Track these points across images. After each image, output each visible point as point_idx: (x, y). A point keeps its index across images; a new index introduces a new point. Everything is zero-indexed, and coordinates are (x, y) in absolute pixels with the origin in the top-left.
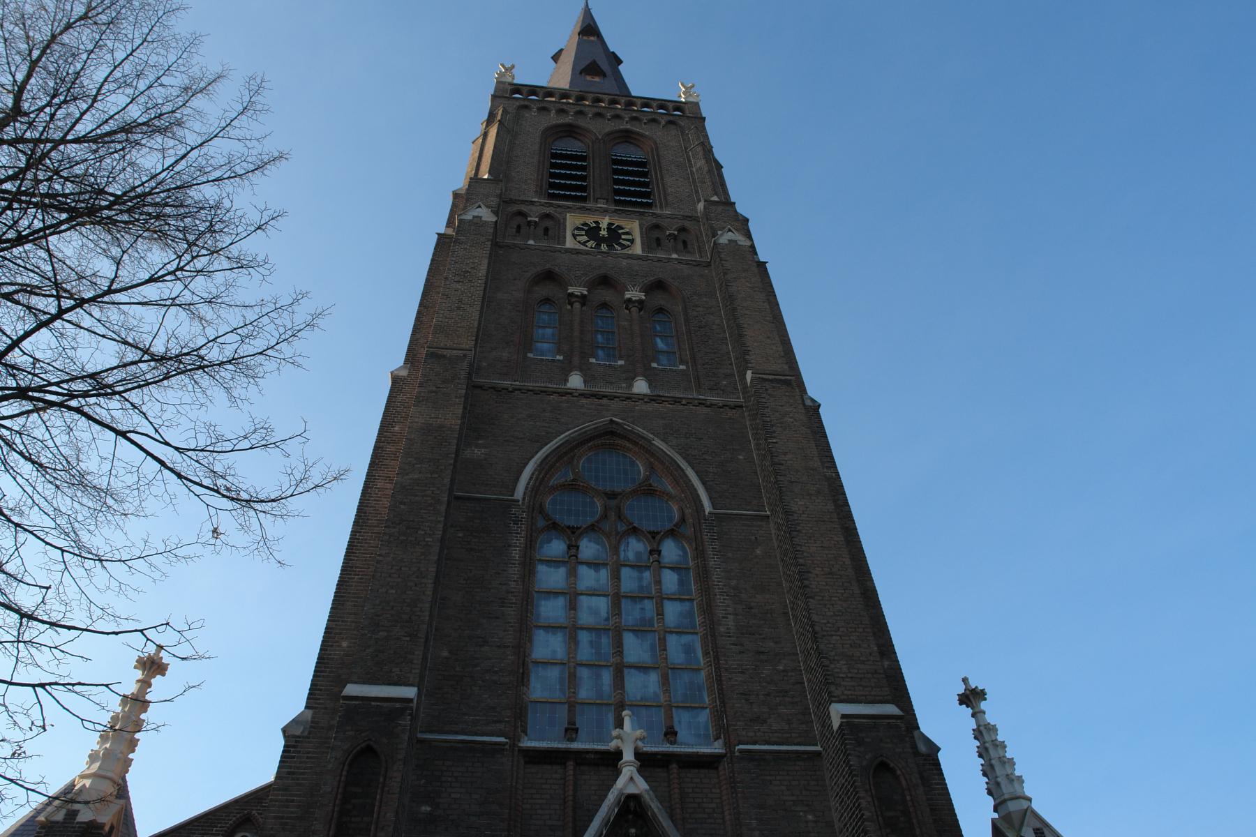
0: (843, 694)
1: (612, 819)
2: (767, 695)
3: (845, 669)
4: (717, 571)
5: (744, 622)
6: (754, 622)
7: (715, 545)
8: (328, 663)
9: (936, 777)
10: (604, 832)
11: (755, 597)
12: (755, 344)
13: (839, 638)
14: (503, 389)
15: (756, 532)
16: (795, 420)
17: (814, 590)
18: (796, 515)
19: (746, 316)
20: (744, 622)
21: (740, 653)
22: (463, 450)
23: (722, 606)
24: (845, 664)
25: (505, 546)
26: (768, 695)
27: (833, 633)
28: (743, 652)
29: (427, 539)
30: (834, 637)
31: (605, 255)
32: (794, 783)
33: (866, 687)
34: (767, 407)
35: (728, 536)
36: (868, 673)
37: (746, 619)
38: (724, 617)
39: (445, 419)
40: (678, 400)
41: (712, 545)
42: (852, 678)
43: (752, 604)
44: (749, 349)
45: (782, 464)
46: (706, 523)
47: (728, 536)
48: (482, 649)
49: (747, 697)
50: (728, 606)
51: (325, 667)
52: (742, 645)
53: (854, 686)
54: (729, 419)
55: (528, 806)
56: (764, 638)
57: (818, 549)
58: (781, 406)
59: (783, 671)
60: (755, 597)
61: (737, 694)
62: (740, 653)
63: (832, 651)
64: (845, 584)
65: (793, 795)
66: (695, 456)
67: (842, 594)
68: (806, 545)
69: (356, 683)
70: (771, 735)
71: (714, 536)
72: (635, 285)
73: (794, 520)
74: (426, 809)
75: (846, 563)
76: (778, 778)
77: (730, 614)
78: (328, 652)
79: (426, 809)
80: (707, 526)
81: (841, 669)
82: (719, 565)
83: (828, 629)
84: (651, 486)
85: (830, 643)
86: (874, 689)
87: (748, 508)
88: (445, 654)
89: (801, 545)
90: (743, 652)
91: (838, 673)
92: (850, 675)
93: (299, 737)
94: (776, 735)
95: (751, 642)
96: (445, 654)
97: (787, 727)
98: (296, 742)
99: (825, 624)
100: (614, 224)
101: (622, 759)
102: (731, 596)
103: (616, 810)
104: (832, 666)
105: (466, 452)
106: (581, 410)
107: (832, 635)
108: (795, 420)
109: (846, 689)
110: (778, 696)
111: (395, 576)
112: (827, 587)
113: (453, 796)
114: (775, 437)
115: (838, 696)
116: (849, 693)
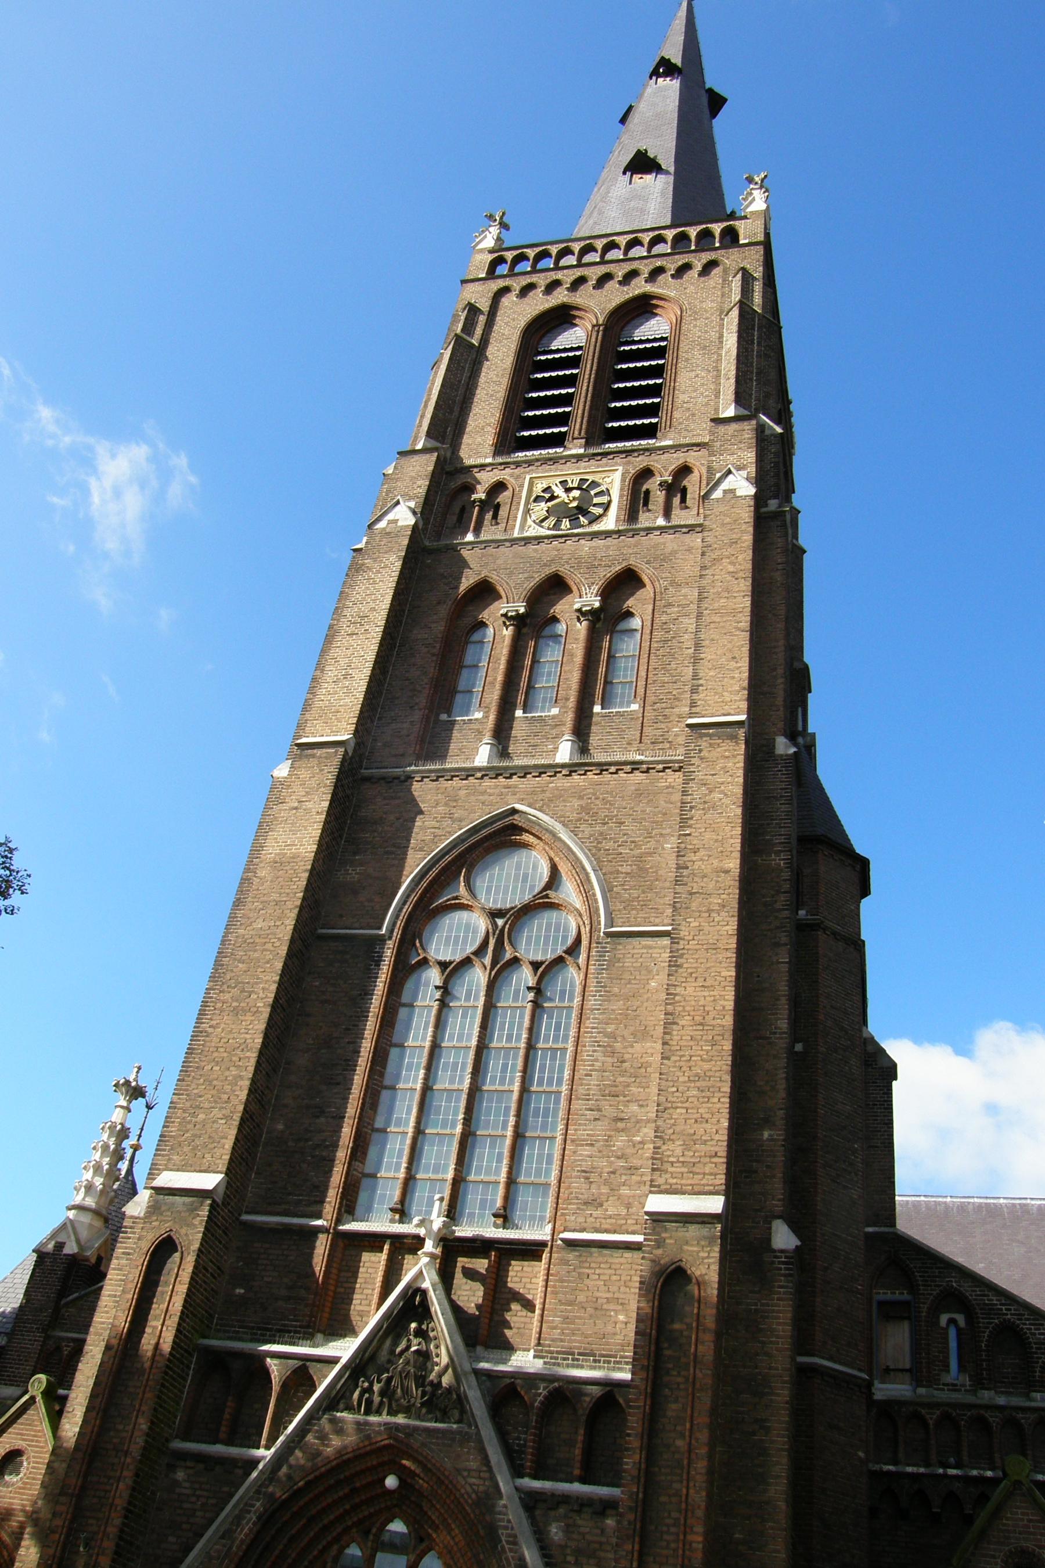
0: (666, 1183)
1: (395, 1312)
2: (612, 1172)
3: (678, 1151)
4: (595, 1014)
5: (610, 1080)
6: (622, 1079)
7: (602, 978)
8: (168, 1141)
9: (783, 1278)
10: (385, 1326)
11: (632, 1047)
12: (712, 673)
13: (684, 1111)
14: (395, 778)
15: (658, 955)
16: (726, 795)
17: (673, 1048)
18: (682, 942)
19: (712, 625)
20: (610, 1080)
21: (596, 1119)
22: (337, 871)
23: (588, 1061)
24: (680, 1145)
25: (361, 995)
26: (613, 1173)
27: (680, 1105)
28: (598, 1119)
29: (258, 1005)
30: (678, 1110)
31: (563, 540)
32: (614, 1278)
33: (698, 1174)
34: (694, 779)
35: (621, 965)
36: (705, 1156)
37: (613, 1075)
38: (586, 1075)
39: (301, 845)
40: (604, 768)
41: (597, 978)
42: (683, 1162)
43: (626, 1056)
44: (701, 682)
45: (687, 868)
46: (598, 947)
47: (621, 965)
48: (317, 1121)
49: (588, 1174)
50: (597, 1060)
51: (166, 1146)
52: (599, 1110)
53: (682, 1173)
54: (668, 787)
55: (342, 1290)
56: (628, 1101)
57: (697, 989)
58: (713, 775)
59: (640, 1143)
60: (632, 1047)
61: (578, 1171)
62: (596, 1119)
63: (670, 1128)
64: (716, 1038)
65: (609, 1291)
66: (609, 850)
67: (708, 1051)
68: (683, 985)
69: (171, 1170)
70: (603, 1221)
71: (603, 965)
72: (593, 584)
73: (678, 950)
74: (240, 1291)
75: (727, 1008)
76: (598, 1271)
77: (596, 1070)
78: (169, 1129)
79: (240, 1291)
80: (598, 952)
81: (673, 1151)
82: (600, 1005)
83: (674, 1099)
84: (549, 898)
85: (672, 1118)
86: (706, 1177)
87: (657, 921)
88: (280, 1127)
89: (675, 986)
90: (598, 1119)
91: (669, 1156)
92: (681, 1159)
93: (136, 1218)
94: (608, 1221)
95: (610, 1106)
96: (280, 1127)
97: (624, 1212)
98: (133, 1223)
99: (673, 1092)
100: (588, 480)
101: (423, 1248)
102: (604, 1046)
103: (401, 1304)
104: (664, 1147)
105: (339, 873)
106: (481, 797)
107: (677, 1108)
108: (726, 795)
109: (672, 1177)
110: (625, 1174)
111: (222, 1050)
112: (692, 1043)
113: (266, 1279)
114: (690, 826)
115: (659, 1186)
116: (674, 1181)
